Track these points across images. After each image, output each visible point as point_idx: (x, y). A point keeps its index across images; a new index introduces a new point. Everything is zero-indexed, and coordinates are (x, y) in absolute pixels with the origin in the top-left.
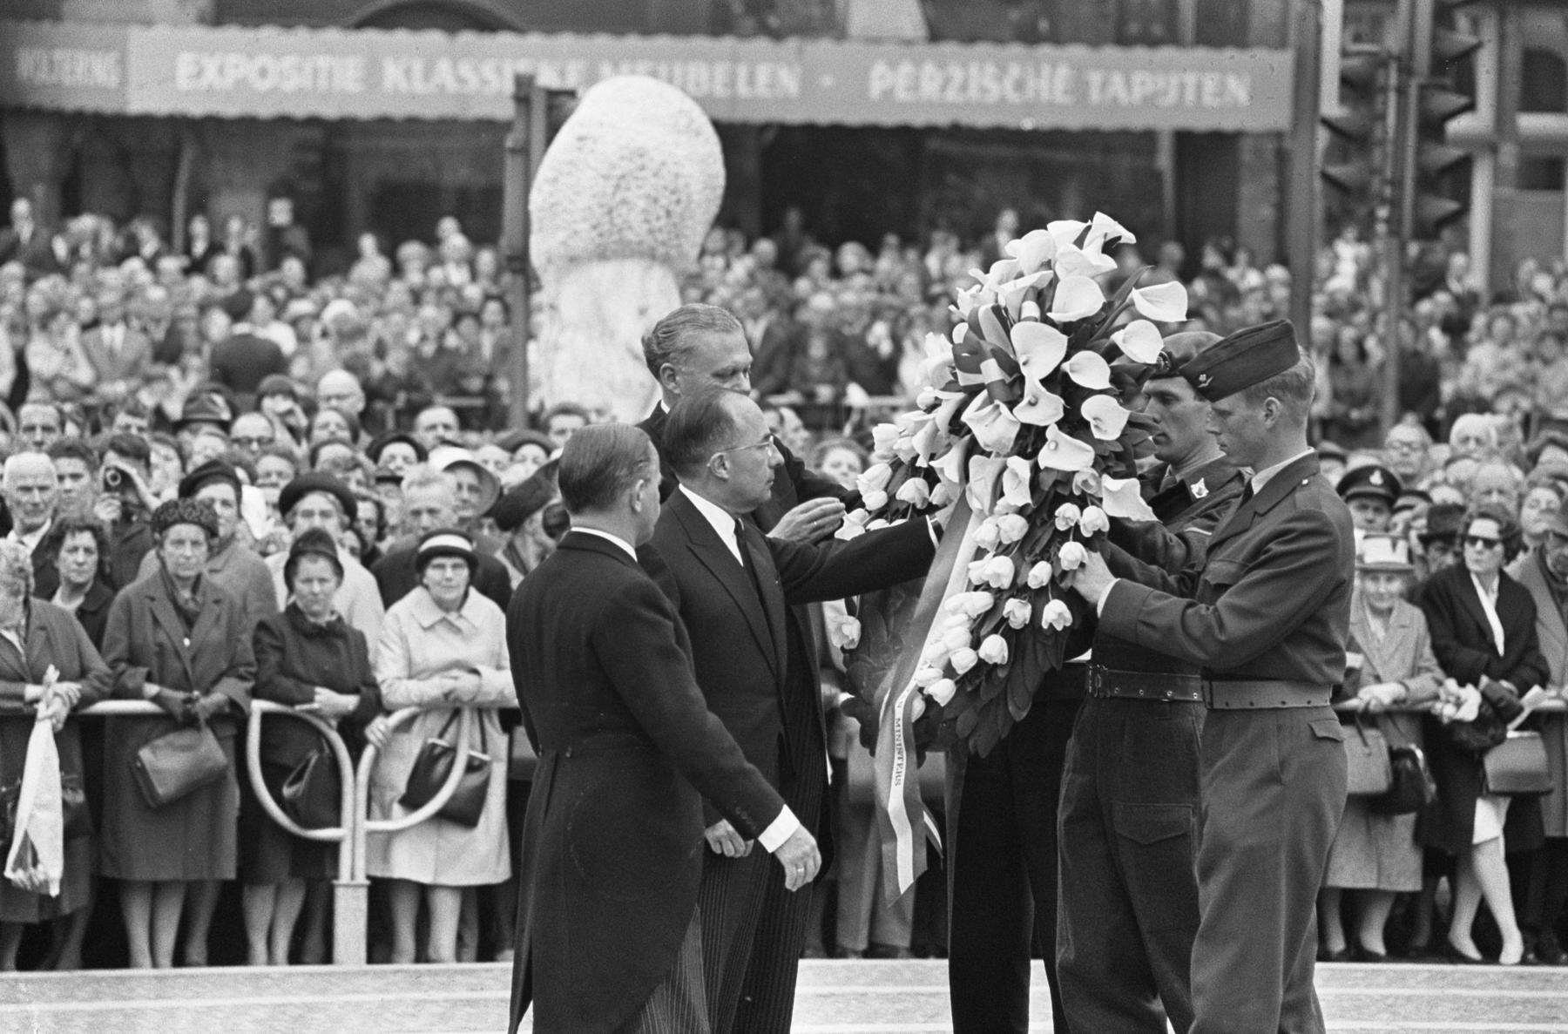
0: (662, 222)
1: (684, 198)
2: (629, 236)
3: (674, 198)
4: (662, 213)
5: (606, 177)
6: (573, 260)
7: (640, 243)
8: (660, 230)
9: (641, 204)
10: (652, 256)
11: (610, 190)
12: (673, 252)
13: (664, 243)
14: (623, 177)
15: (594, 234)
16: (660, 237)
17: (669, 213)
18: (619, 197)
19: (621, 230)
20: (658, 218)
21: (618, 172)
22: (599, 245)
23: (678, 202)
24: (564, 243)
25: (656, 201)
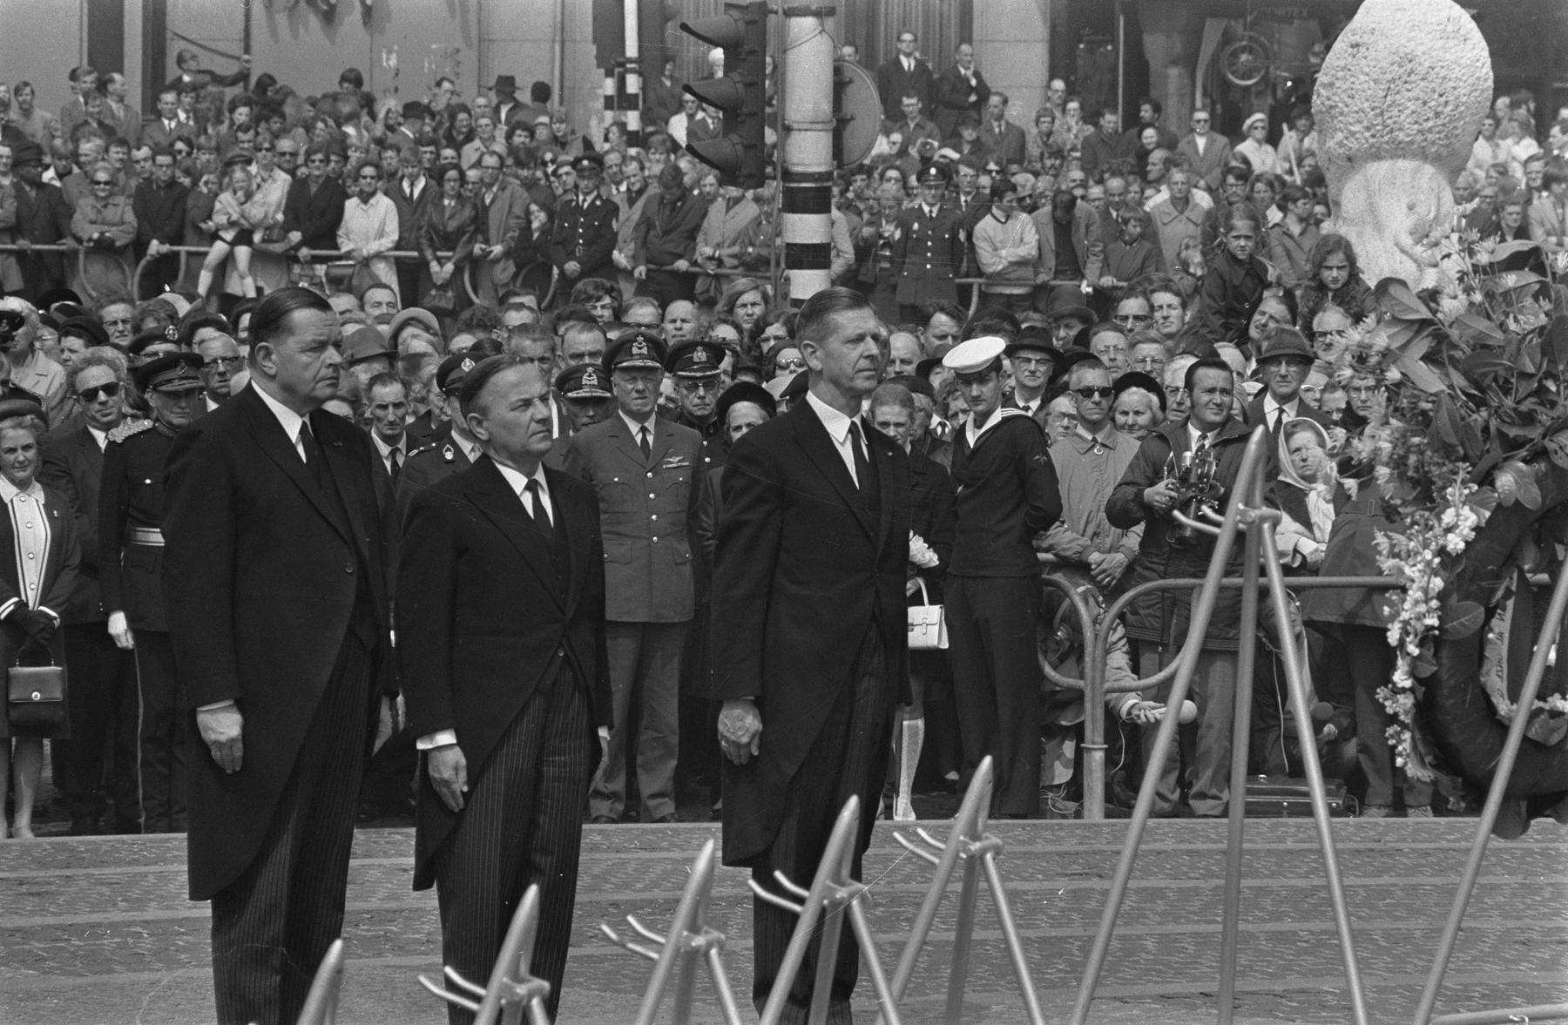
0: (1430, 124)
2: (1401, 136)
3: (1443, 99)
5: (1376, 81)
6: (1349, 159)
7: (1412, 142)
8: (1430, 130)
9: (1411, 106)
12: (1444, 152)
13: (1433, 143)
14: (1393, 80)
15: (1367, 134)
17: (1437, 115)
19: (1391, 131)
21: (1389, 77)
22: (1372, 145)
24: (1341, 144)
25: (1425, 103)
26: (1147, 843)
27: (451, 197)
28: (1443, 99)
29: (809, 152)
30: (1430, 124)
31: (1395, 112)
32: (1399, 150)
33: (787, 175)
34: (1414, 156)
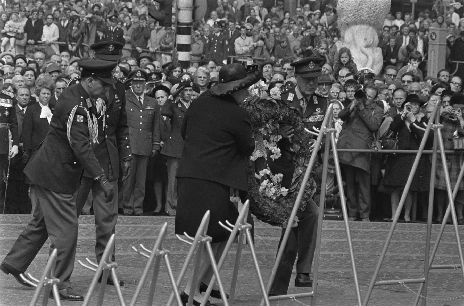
0: (372, 15)
1: (378, 7)
2: (363, 18)
3: (376, 7)
4: (372, 12)
6: (347, 24)
7: (366, 20)
8: (372, 17)
9: (366, 9)
10: (370, 25)
11: (358, 5)
12: (376, 23)
13: (373, 20)
15: (353, 17)
16: (372, 18)
17: (374, 12)
18: (360, 7)
19: (360, 16)
20: (371, 13)
22: (354, 21)
23: (377, 9)
24: (345, 20)
25: (371, 8)
26: (443, 240)
27: (76, 26)
28: (376, 7)
29: (185, 17)
30: (372, 15)
31: (362, 11)
32: (362, 22)
33: (178, 23)
34: (367, 24)
